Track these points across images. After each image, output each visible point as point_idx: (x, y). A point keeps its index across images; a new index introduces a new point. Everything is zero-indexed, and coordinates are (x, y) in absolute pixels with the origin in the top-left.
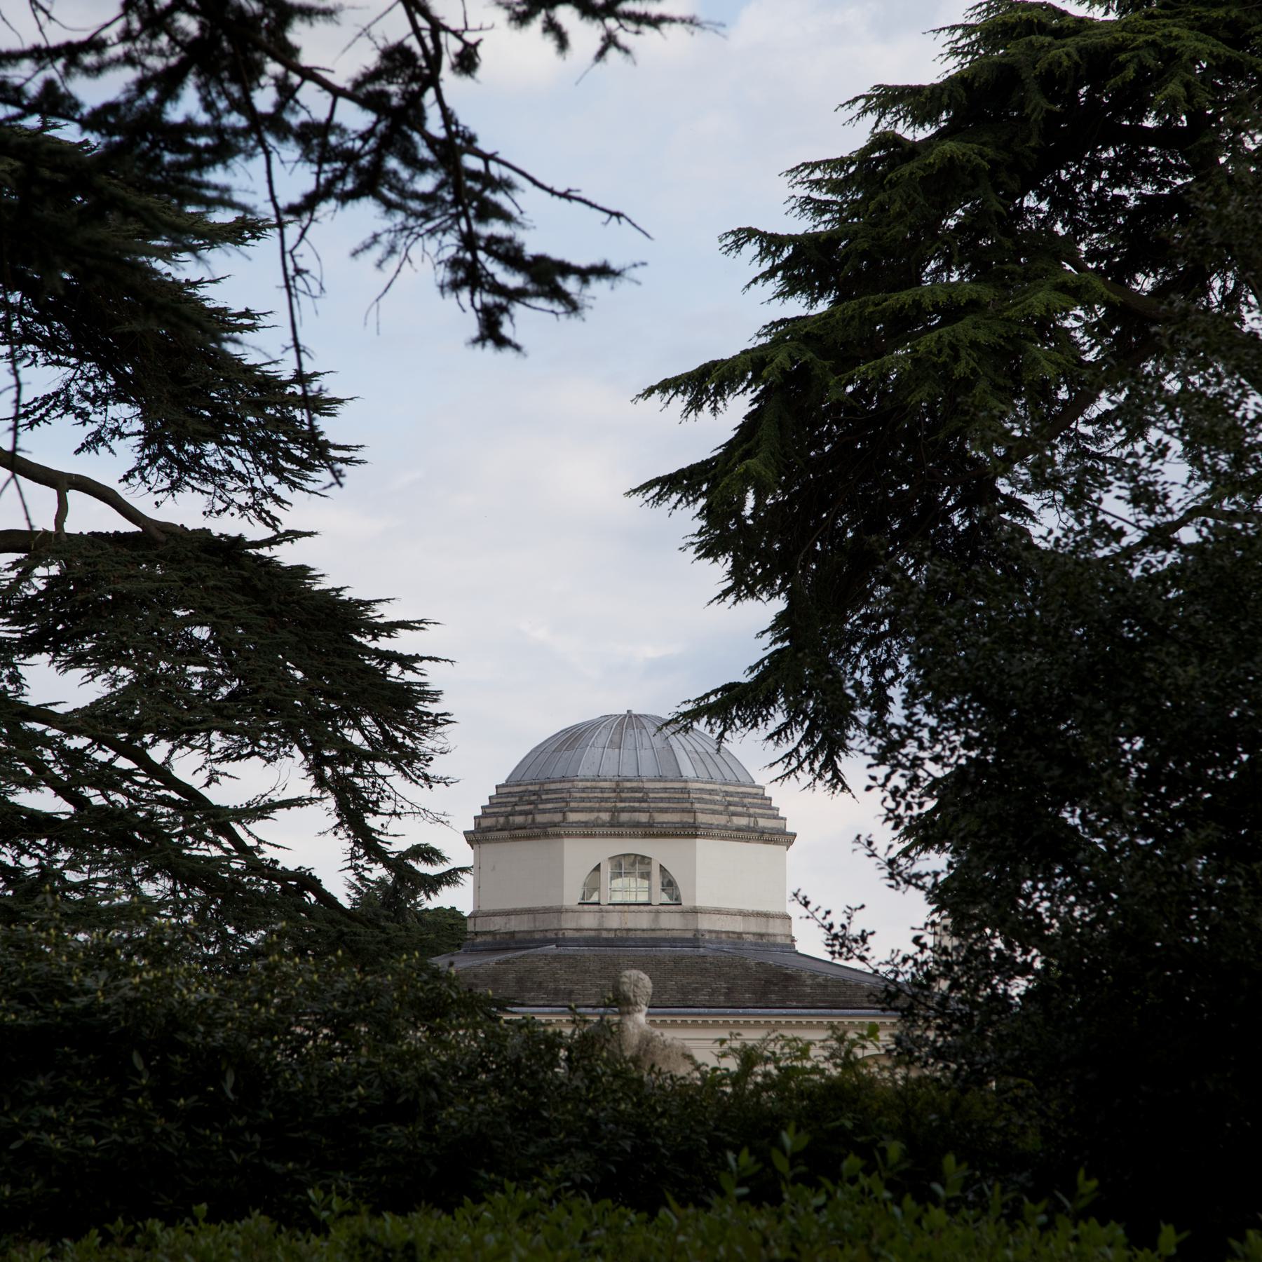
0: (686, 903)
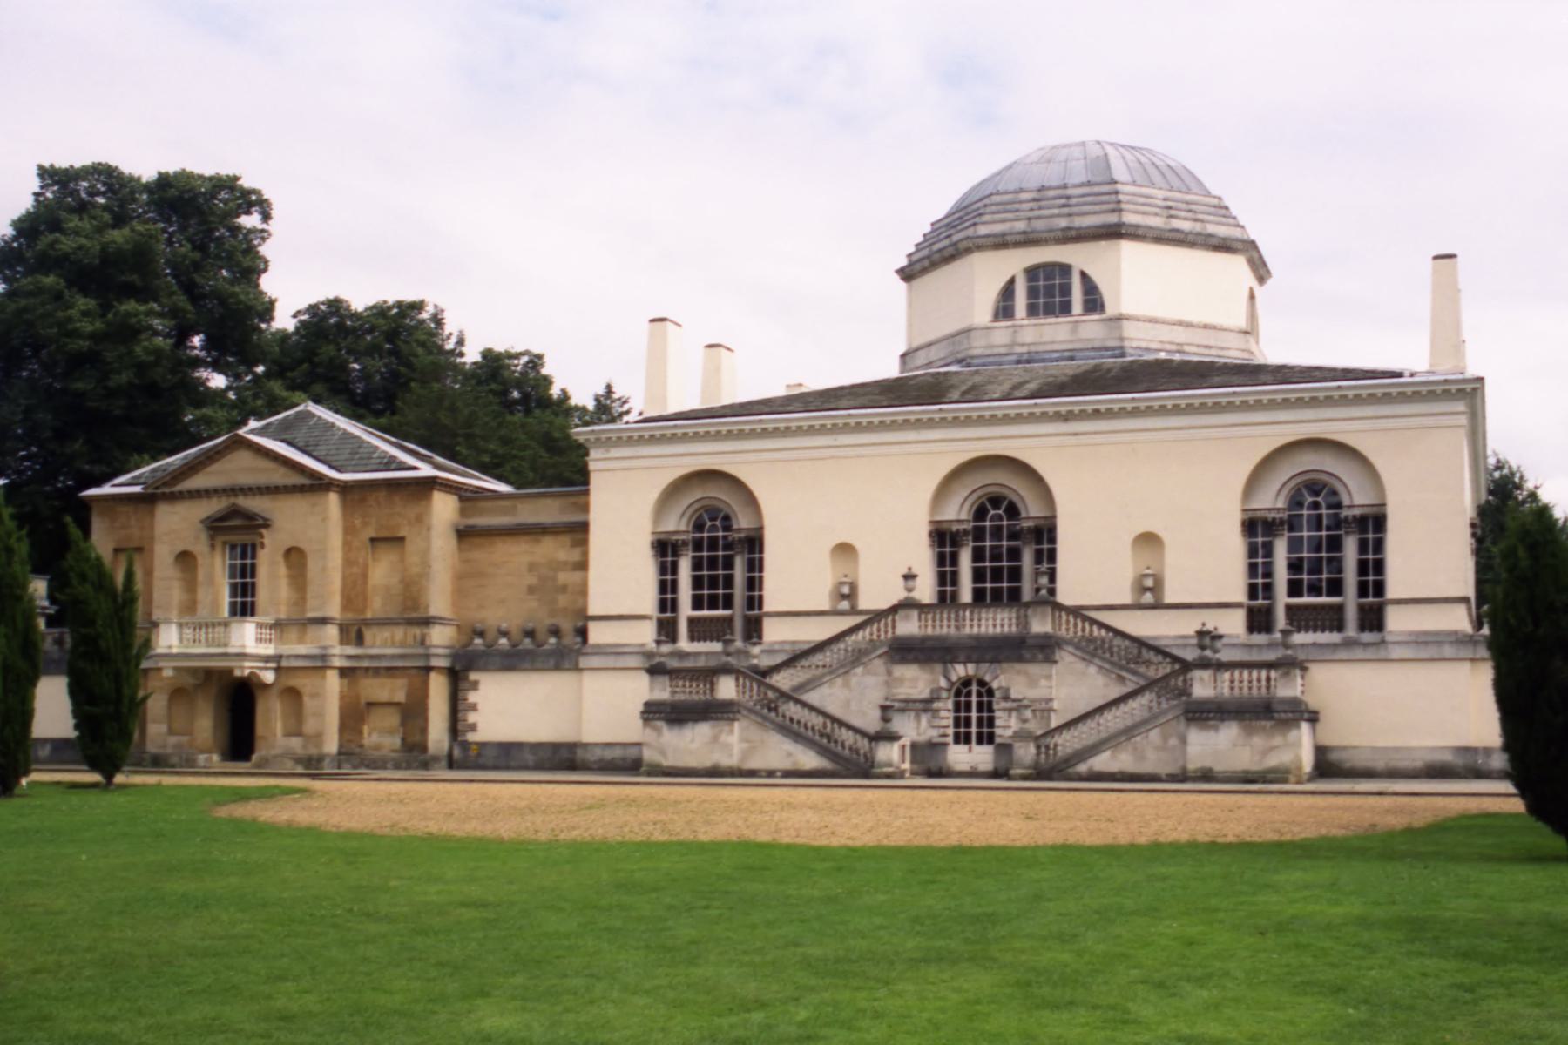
0: (1110, 310)
